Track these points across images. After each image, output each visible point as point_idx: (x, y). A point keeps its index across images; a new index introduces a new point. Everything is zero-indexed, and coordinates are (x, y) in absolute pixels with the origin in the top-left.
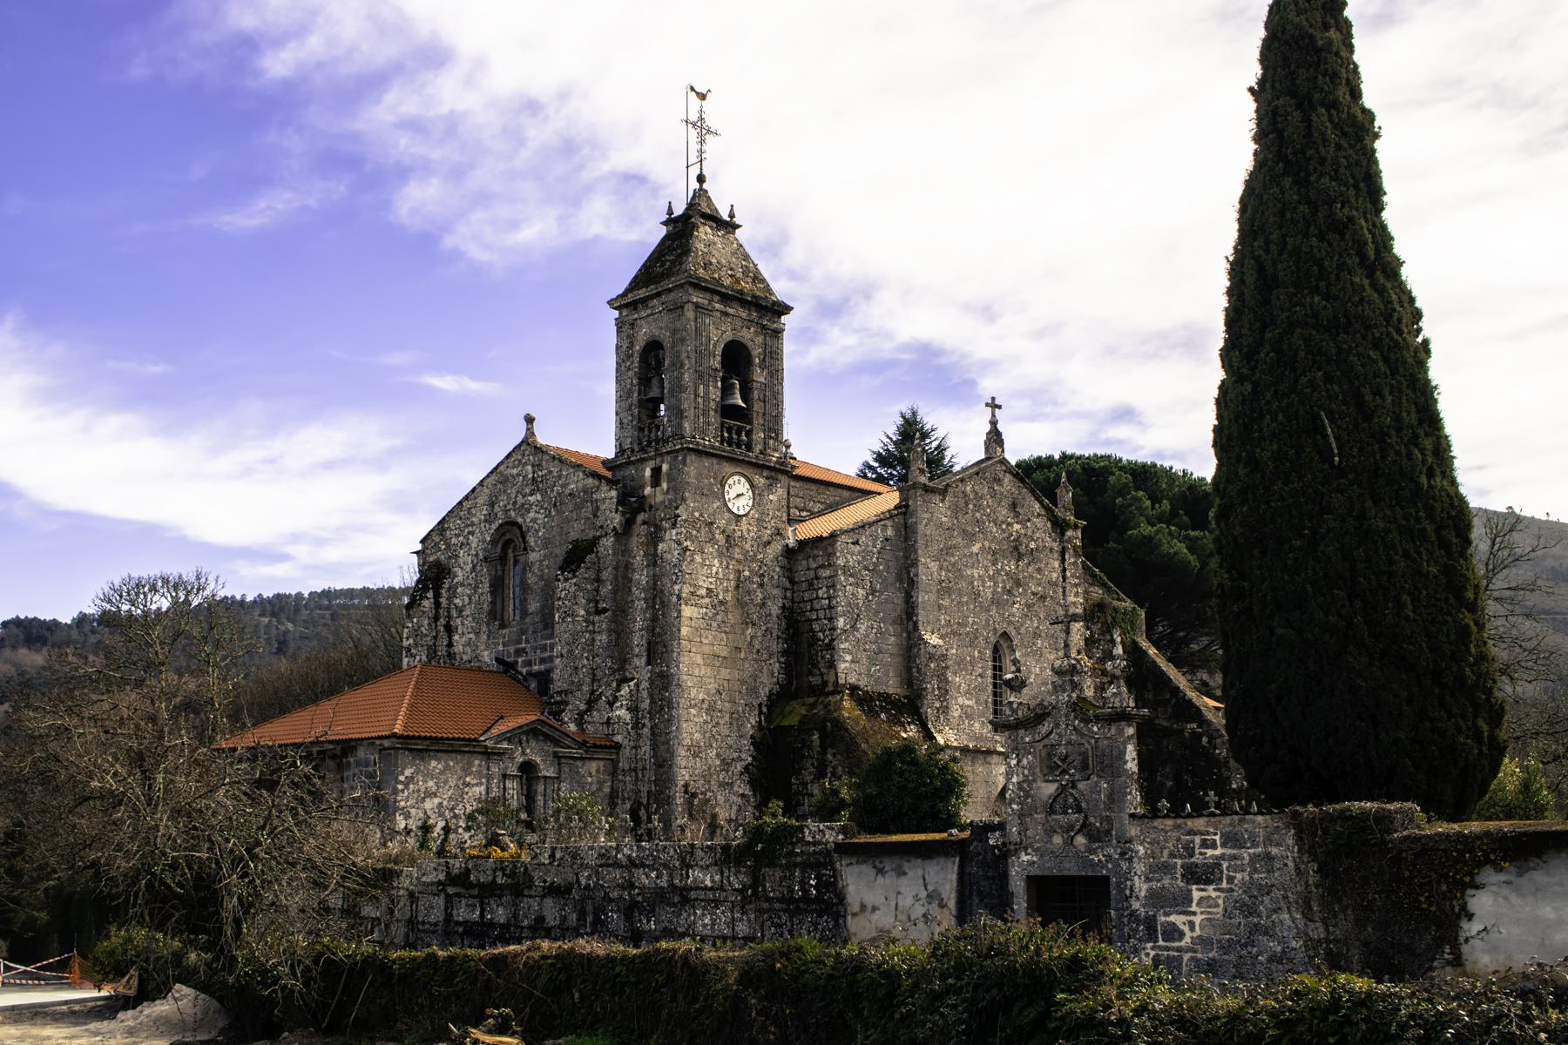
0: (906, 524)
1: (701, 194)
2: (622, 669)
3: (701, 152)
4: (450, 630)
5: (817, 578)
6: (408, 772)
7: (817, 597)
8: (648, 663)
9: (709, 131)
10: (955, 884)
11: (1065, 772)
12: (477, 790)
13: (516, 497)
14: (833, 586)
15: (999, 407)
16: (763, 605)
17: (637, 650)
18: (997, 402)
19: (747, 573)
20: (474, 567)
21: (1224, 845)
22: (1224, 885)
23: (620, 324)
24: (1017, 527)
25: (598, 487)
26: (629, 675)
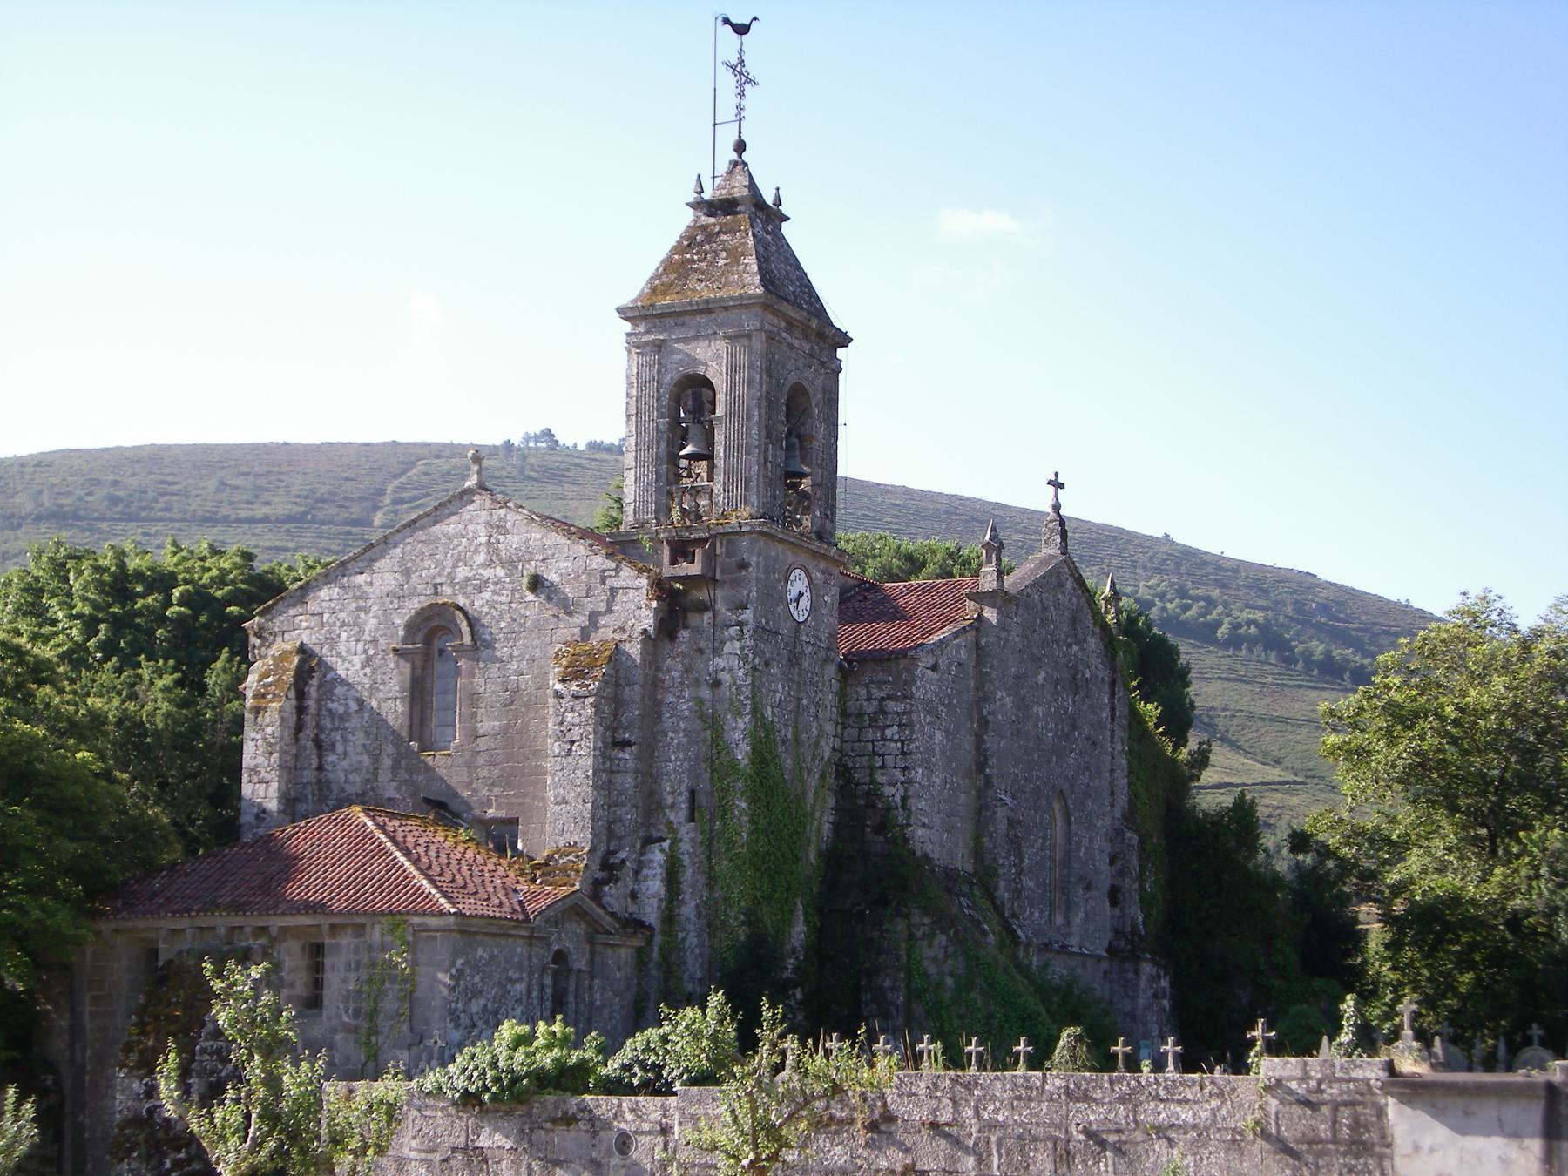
0: (977, 643)
3: (740, 108)
5: (882, 711)
7: (884, 739)
8: (692, 819)
9: (748, 80)
13: (455, 566)
14: (911, 725)
15: (1062, 486)
17: (670, 800)
18: (1060, 480)
19: (805, 702)
24: (1075, 648)
26: (656, 834)
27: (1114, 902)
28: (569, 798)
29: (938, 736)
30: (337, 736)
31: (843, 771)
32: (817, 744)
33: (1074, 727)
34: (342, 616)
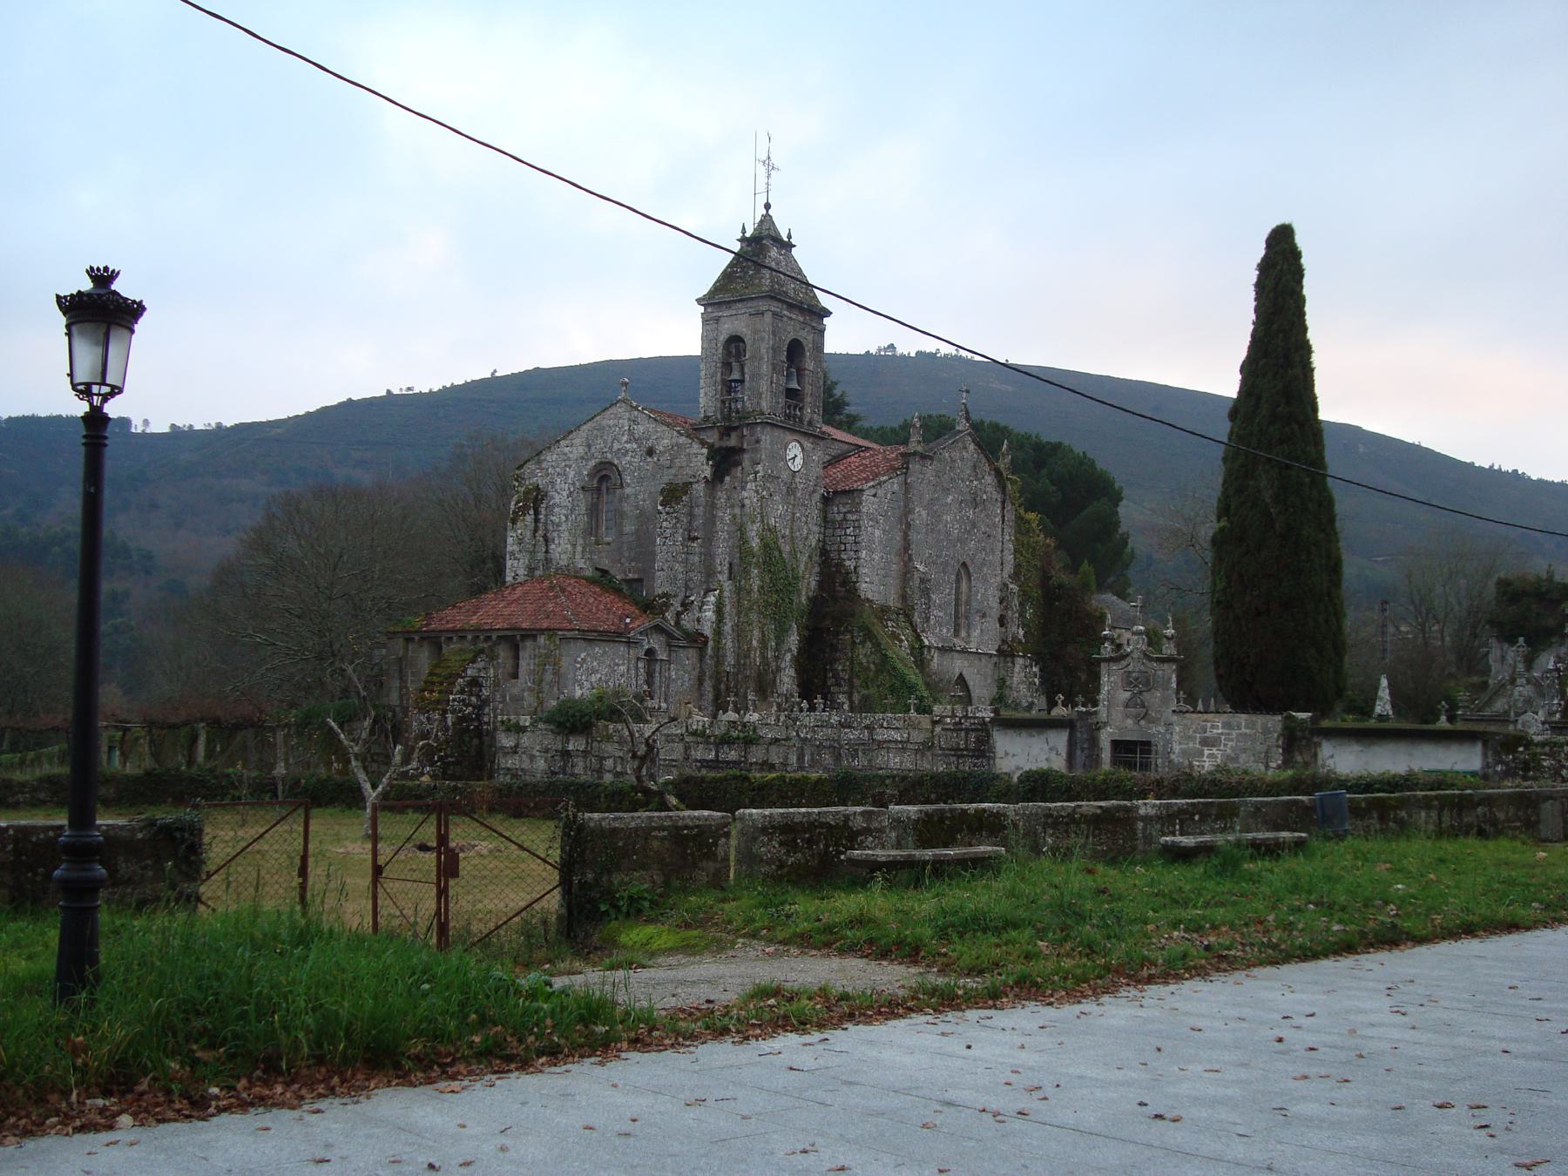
0: (906, 483)
1: (767, 220)
2: (707, 582)
4: (546, 540)
5: (845, 519)
6: (583, 655)
7: (846, 534)
10: (1066, 744)
11: (1136, 686)
12: (622, 668)
13: (613, 443)
14: (859, 527)
16: (806, 539)
19: (798, 515)
20: (571, 492)
21: (1223, 728)
22: (1222, 748)
23: (706, 321)
24: (975, 483)
25: (691, 444)
26: (712, 587)
27: (1002, 625)
28: (665, 568)
29: (877, 533)
30: (555, 534)
31: (824, 553)
32: (806, 539)
33: (974, 526)
34: (558, 470)
